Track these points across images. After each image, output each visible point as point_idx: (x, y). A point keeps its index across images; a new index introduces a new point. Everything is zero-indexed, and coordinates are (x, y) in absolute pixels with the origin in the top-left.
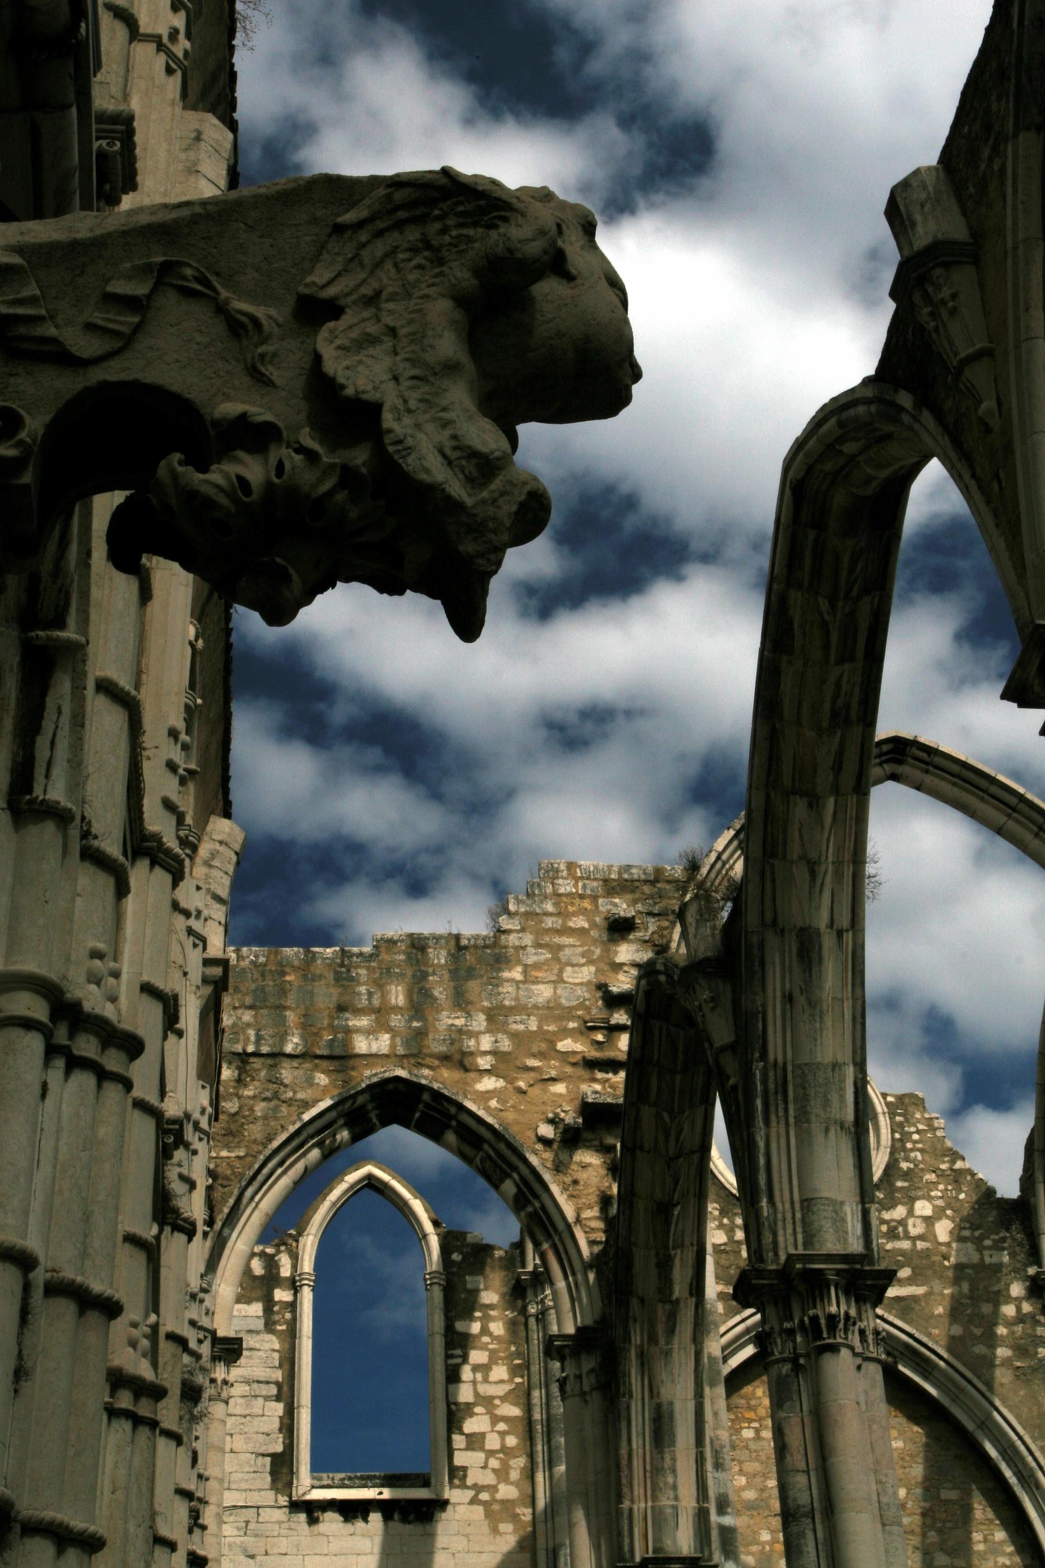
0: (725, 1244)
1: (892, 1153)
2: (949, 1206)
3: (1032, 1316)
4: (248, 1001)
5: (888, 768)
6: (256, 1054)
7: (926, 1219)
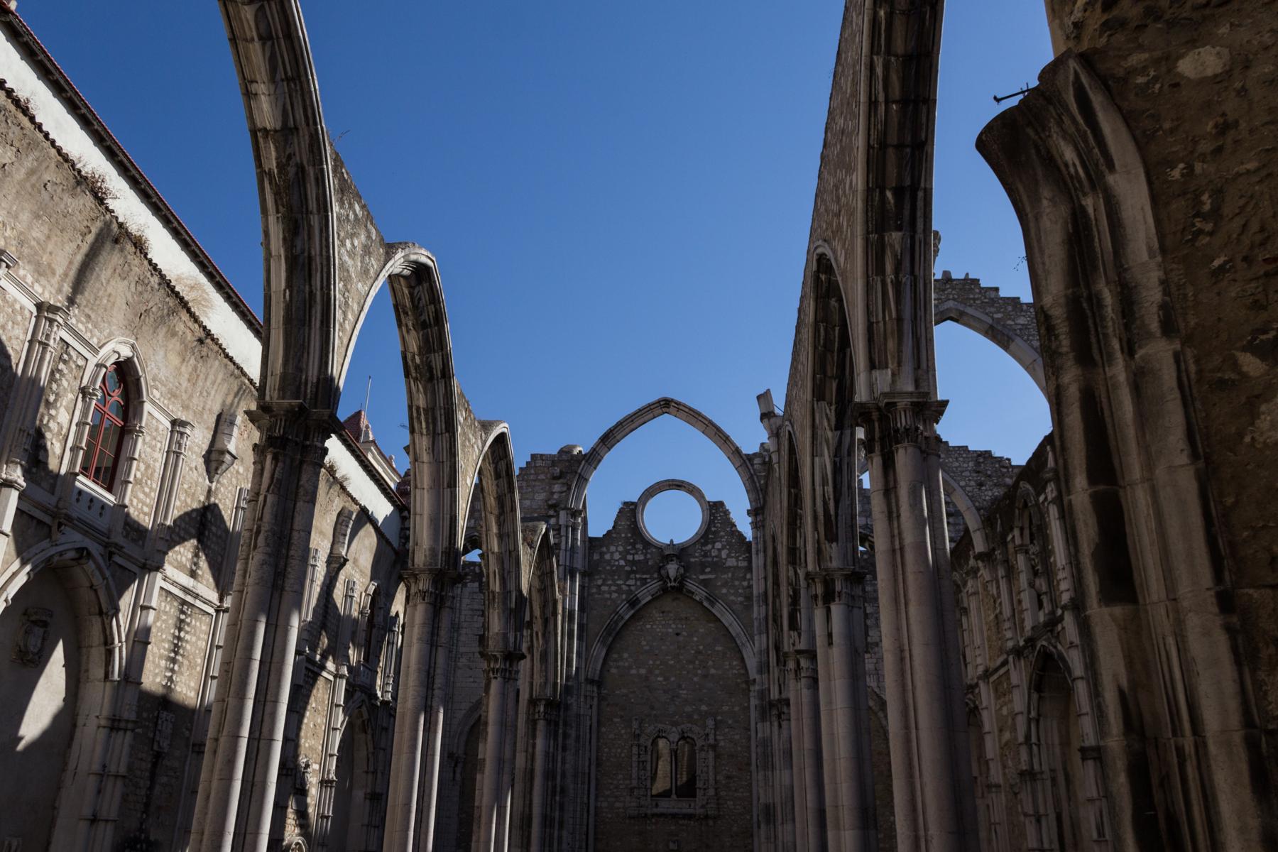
7: (719, 550)
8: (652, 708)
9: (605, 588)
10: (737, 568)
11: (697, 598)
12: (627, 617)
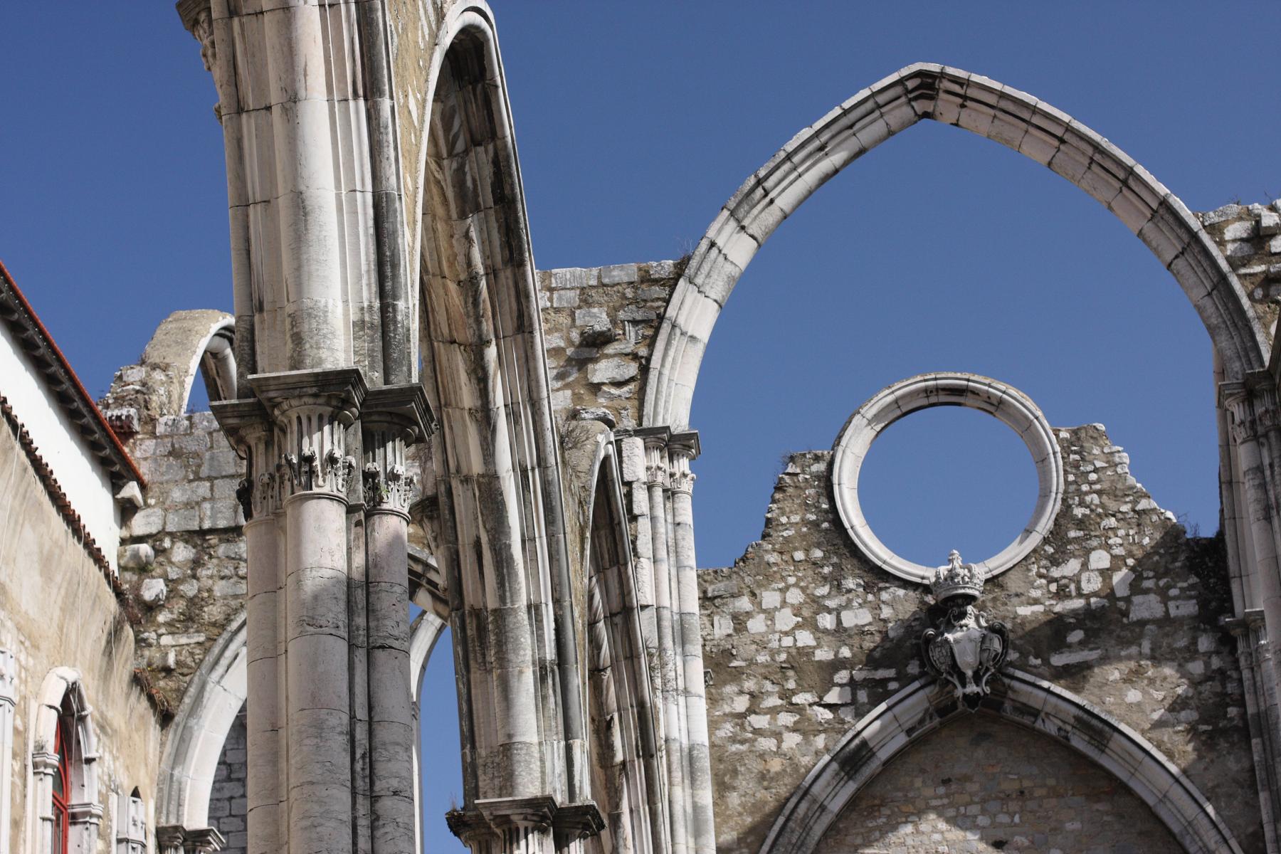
0: (870, 624)
1: (1064, 500)
2: (1130, 554)
3: (1221, 672)
4: (205, 471)
5: (920, 106)
6: (212, 531)
7: (1105, 574)
10: (1166, 621)
11: (1051, 727)
12: (836, 805)
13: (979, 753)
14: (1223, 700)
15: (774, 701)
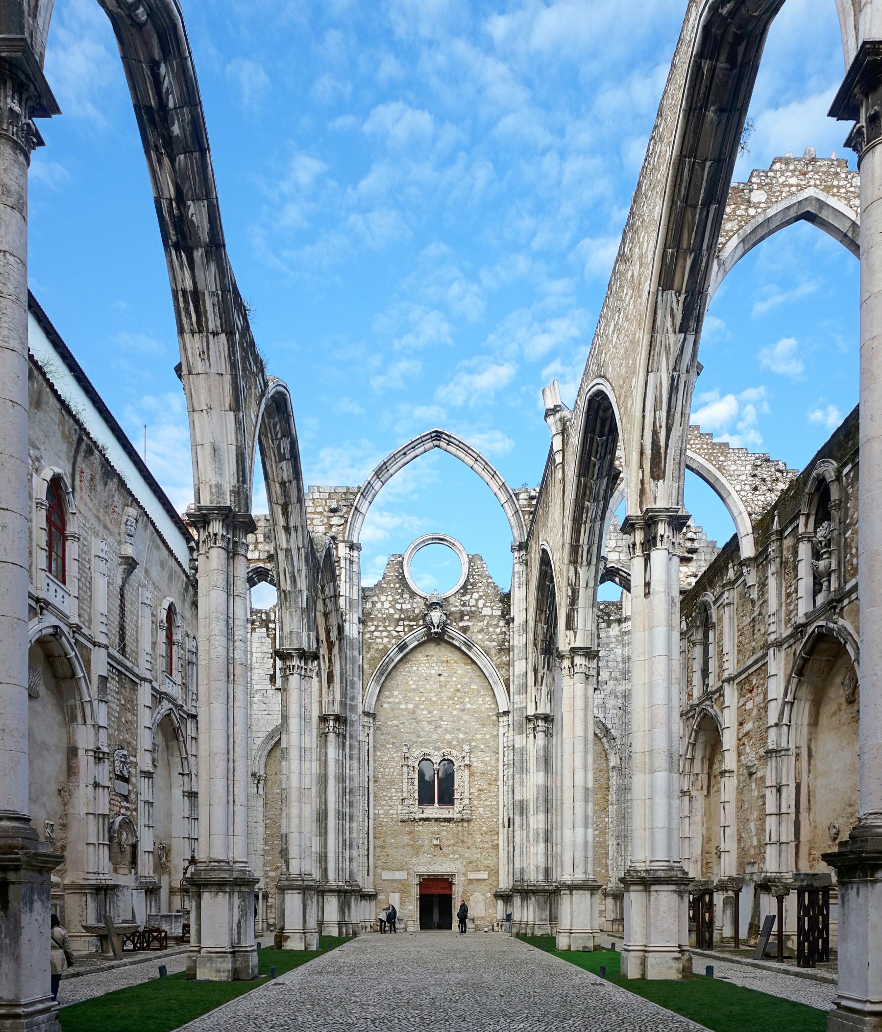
8: (419, 736)
9: (376, 634)
10: (491, 616)
11: (457, 644)
12: (396, 660)
13: (437, 649)
14: (504, 640)
15: (381, 628)
